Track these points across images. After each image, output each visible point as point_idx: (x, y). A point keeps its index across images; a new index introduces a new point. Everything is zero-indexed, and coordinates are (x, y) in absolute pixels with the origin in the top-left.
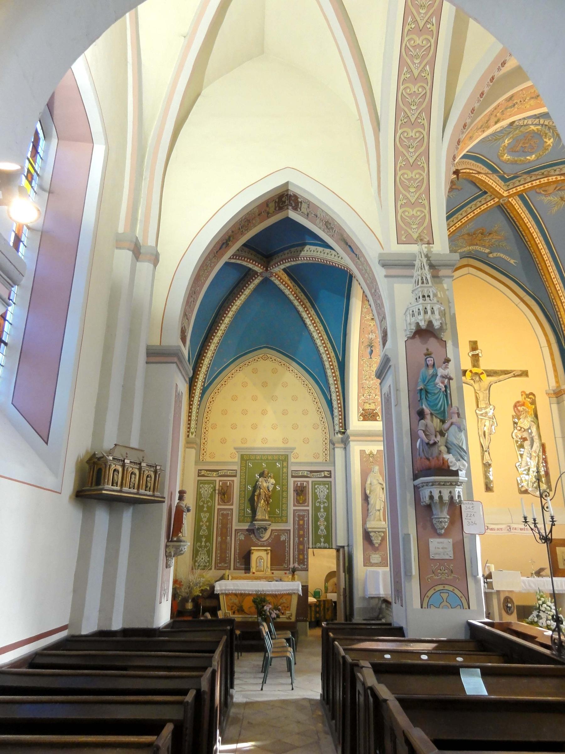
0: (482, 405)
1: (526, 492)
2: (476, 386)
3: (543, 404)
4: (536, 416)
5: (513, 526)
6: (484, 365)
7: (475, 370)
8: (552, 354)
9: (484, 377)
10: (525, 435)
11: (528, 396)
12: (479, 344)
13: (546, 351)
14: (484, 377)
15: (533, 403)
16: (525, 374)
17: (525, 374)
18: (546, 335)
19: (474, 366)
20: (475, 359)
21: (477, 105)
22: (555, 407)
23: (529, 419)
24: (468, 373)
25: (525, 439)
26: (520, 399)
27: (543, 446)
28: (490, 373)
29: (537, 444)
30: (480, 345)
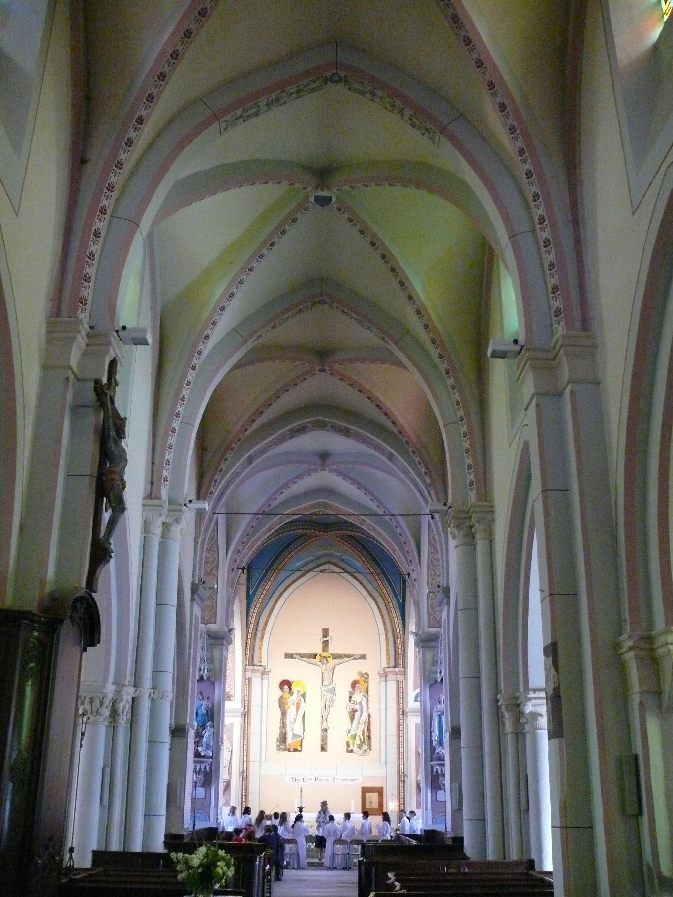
0: (326, 683)
1: (352, 751)
2: (323, 667)
3: (374, 682)
4: (367, 692)
5: (337, 777)
6: (333, 649)
7: (324, 654)
8: (387, 640)
9: (330, 659)
10: (357, 707)
11: (363, 675)
12: (330, 632)
13: (383, 637)
14: (330, 659)
15: (366, 681)
16: (363, 657)
17: (363, 657)
18: (384, 624)
19: (324, 651)
20: (326, 644)
21: (245, 540)
22: (383, 684)
23: (361, 694)
24: (318, 657)
25: (356, 711)
26: (357, 677)
27: (369, 716)
28: (336, 657)
29: (364, 716)
30: (330, 633)
